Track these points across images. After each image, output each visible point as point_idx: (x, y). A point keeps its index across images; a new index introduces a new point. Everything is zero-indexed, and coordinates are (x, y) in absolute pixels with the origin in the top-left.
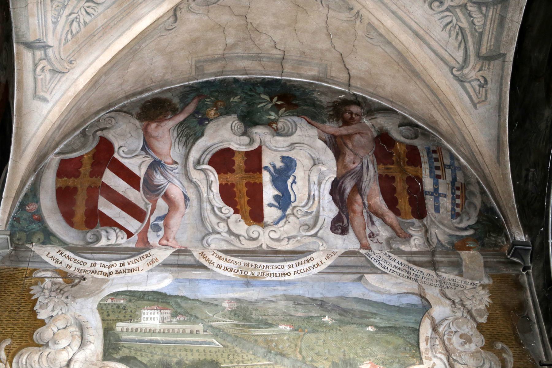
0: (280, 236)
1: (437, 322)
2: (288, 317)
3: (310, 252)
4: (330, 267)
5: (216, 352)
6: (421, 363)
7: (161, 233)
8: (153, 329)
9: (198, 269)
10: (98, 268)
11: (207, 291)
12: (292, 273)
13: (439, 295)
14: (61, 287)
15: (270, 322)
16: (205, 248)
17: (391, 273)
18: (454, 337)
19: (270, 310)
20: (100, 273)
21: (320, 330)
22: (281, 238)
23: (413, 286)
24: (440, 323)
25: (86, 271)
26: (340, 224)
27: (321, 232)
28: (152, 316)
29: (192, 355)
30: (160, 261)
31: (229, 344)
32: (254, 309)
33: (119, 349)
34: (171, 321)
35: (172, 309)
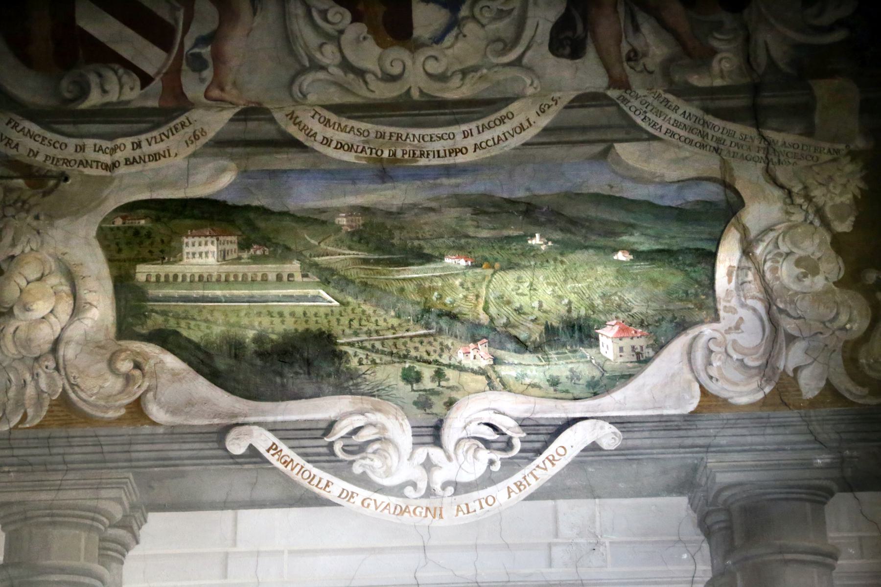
0: (447, 69)
1: (753, 234)
2: (463, 241)
3: (508, 101)
4: (546, 130)
5: (327, 315)
6: (717, 319)
7: (208, 74)
8: (205, 276)
9: (286, 149)
10: (90, 154)
11: (305, 197)
12: (471, 149)
13: (762, 181)
14: (24, 197)
15: (426, 251)
16: (296, 102)
17: (667, 137)
18: (785, 264)
19: (427, 228)
20: (94, 164)
21: (524, 262)
22: (449, 74)
23: (710, 165)
24: (759, 239)
25: (67, 162)
26: (569, 34)
27: (529, 54)
28: (203, 249)
29: (283, 322)
30: (211, 135)
31: (350, 299)
32: (396, 228)
33: (145, 315)
34: (240, 258)
35: (240, 233)
